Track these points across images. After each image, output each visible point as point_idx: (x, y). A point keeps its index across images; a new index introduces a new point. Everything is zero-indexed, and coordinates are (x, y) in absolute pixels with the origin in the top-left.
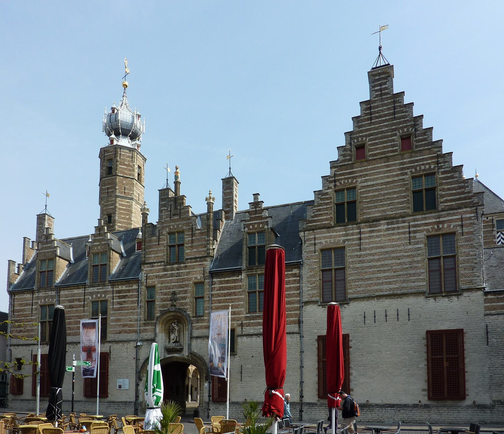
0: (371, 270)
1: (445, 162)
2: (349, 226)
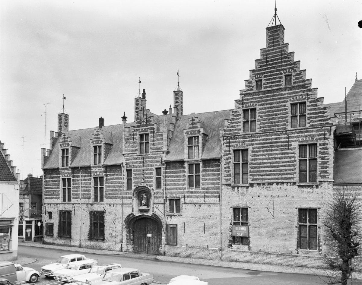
1: (312, 95)
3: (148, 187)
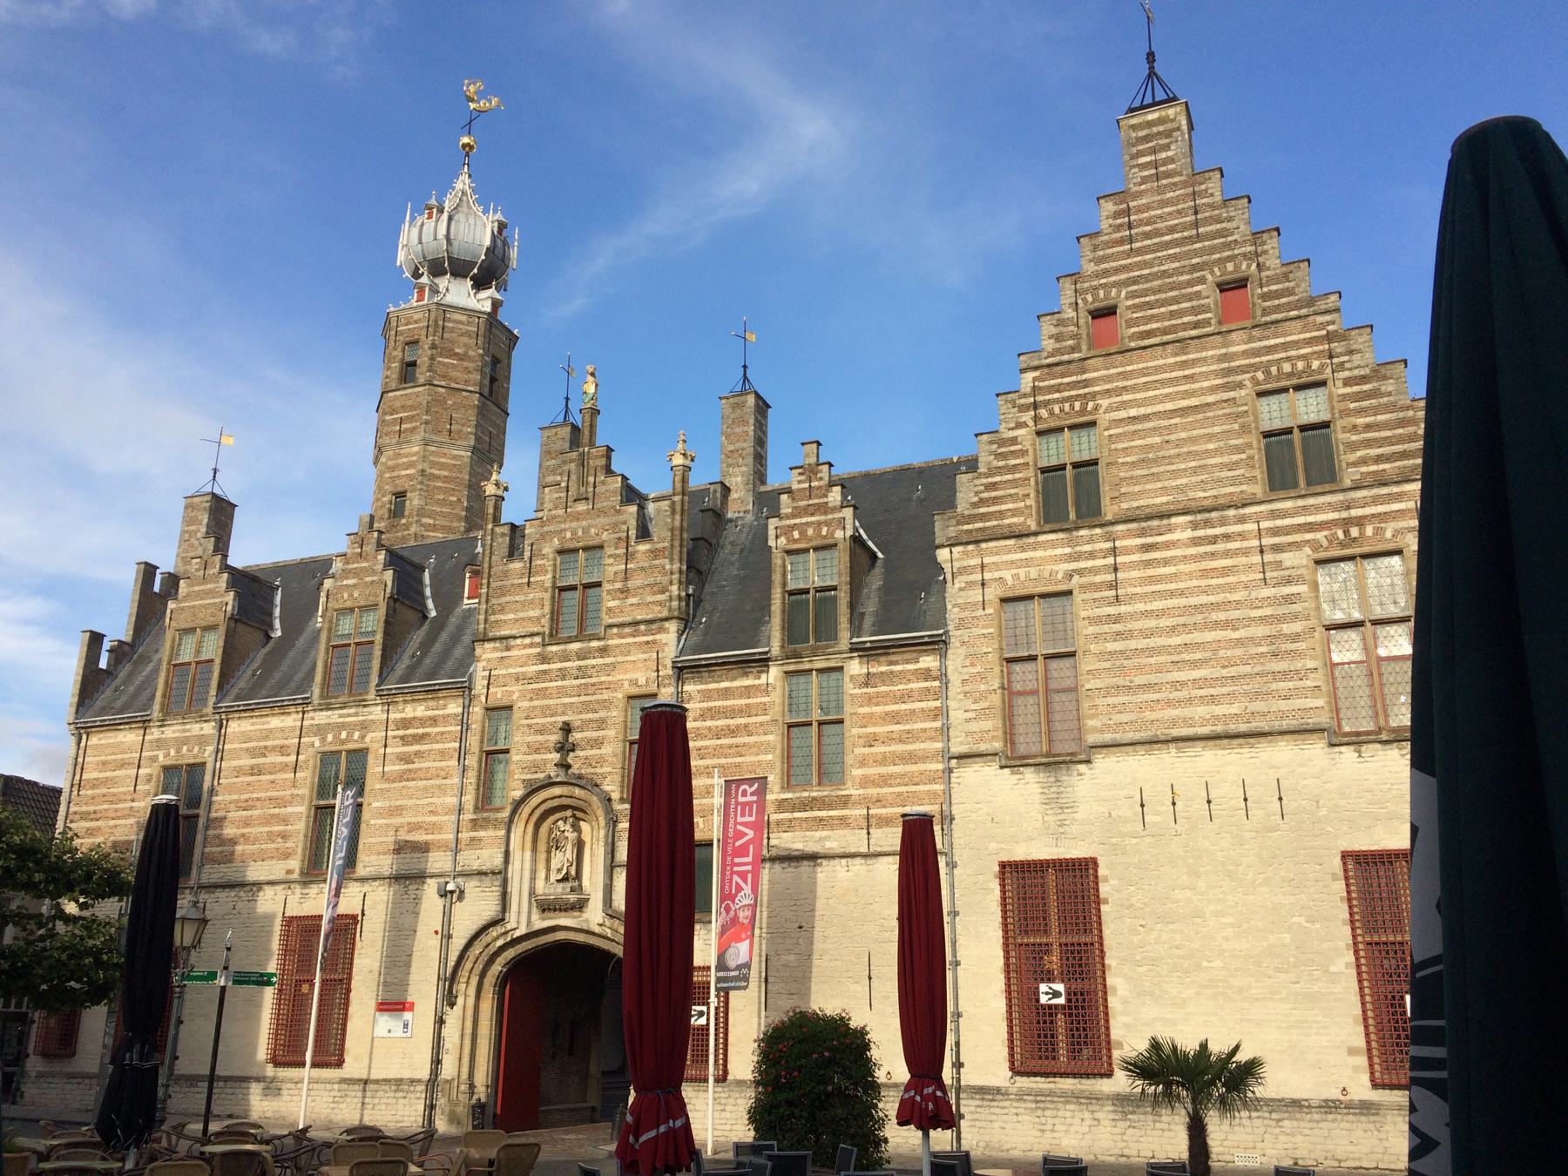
0: (1152, 660)
1: (1351, 352)
2: (1082, 532)
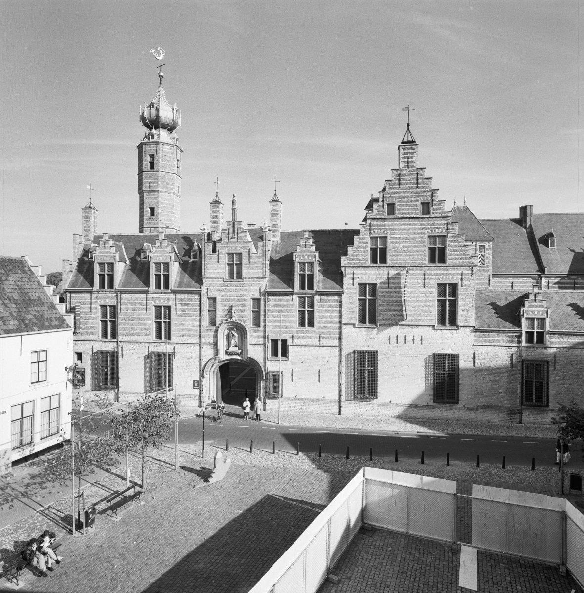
1: (452, 229)
3: (242, 323)
